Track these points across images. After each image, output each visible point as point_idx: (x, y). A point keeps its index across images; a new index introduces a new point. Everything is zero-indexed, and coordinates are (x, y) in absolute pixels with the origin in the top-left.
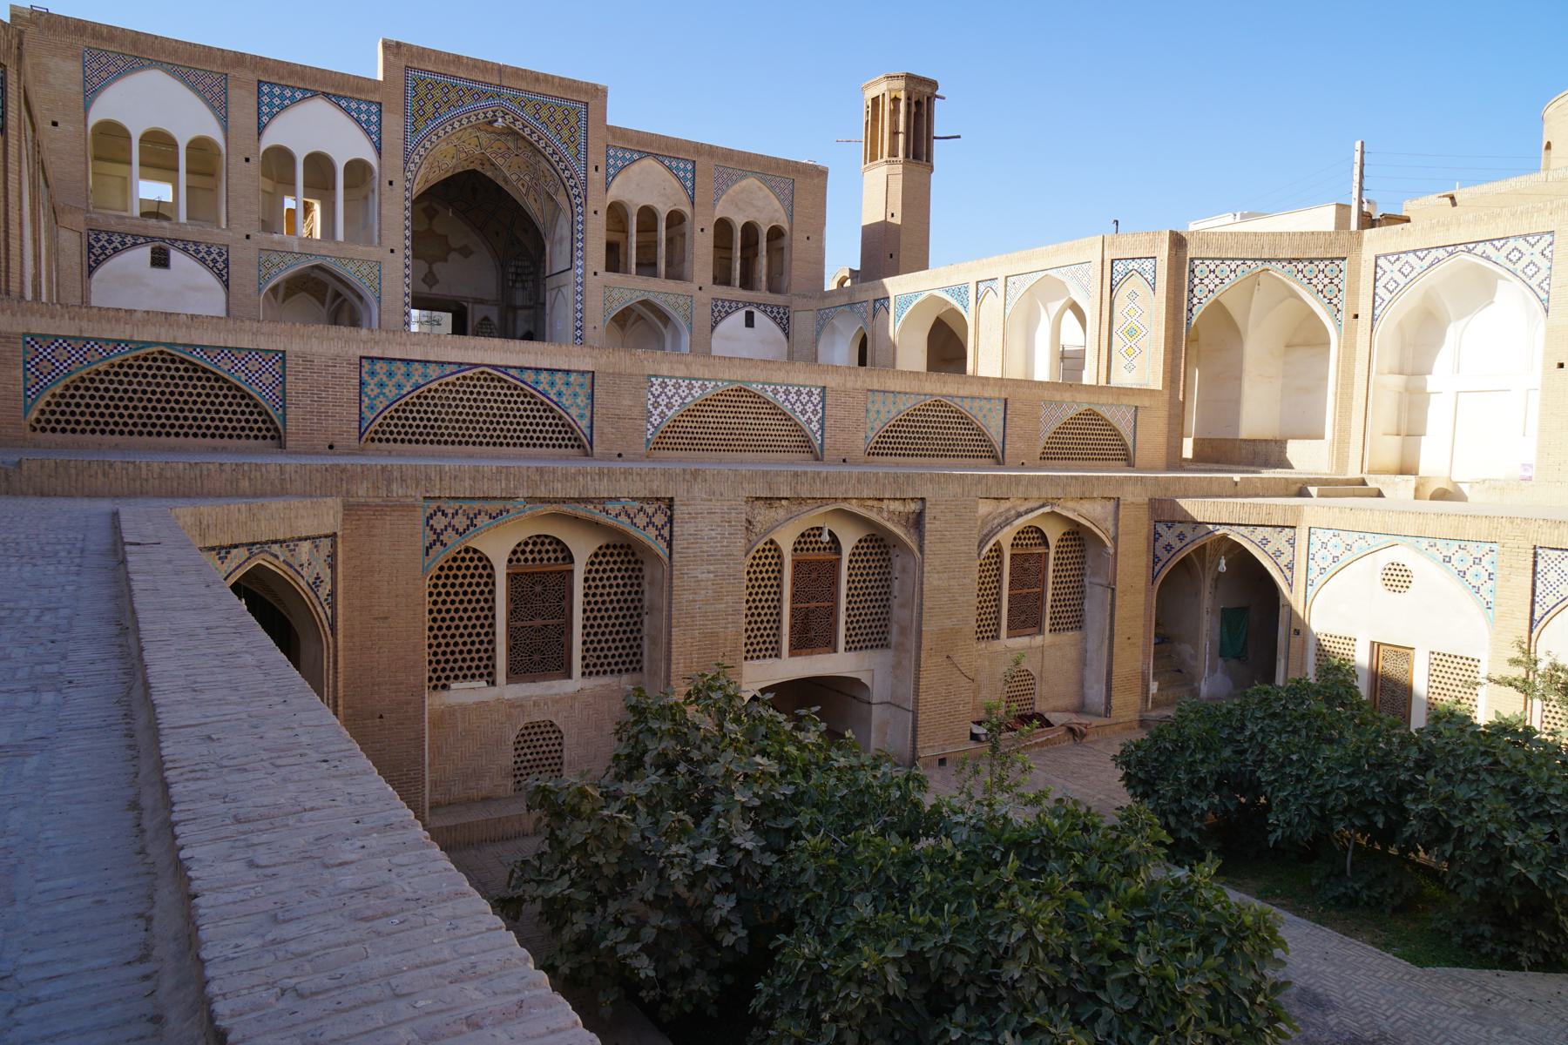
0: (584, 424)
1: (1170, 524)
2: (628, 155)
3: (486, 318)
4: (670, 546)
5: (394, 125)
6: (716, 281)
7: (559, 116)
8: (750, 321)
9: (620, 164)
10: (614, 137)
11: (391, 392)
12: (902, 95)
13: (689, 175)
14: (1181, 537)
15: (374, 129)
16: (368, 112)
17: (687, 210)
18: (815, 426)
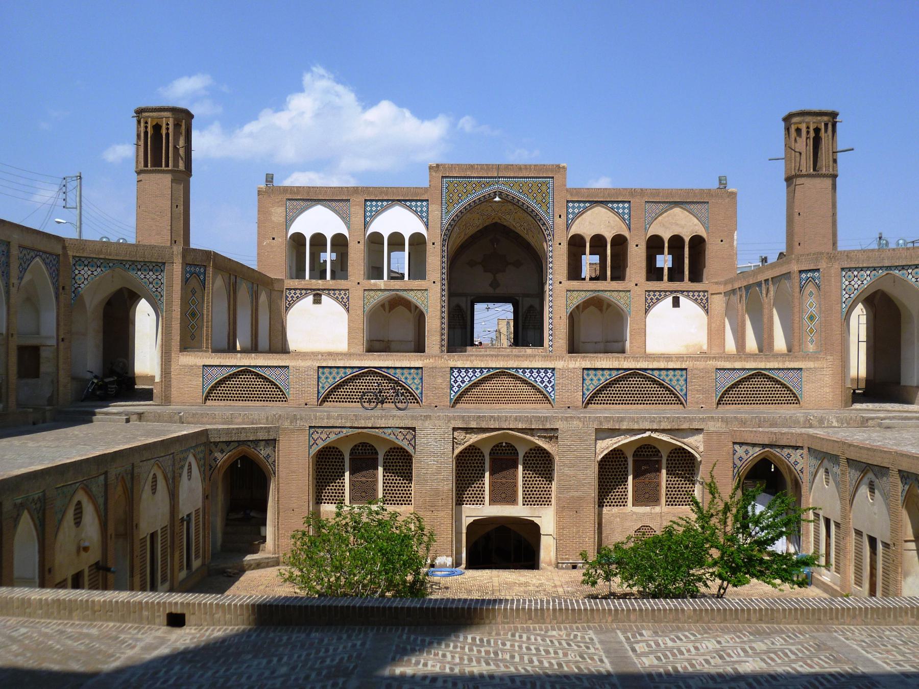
0: (418, 392)
1: (741, 444)
2: (582, 205)
3: (531, 307)
4: (414, 448)
5: (435, 211)
6: (649, 279)
7: (535, 189)
8: (676, 303)
9: (576, 211)
10: (572, 195)
11: (331, 381)
12: (803, 127)
13: (626, 211)
14: (747, 452)
15: (424, 214)
16: (422, 206)
17: (626, 234)
18: (550, 389)
